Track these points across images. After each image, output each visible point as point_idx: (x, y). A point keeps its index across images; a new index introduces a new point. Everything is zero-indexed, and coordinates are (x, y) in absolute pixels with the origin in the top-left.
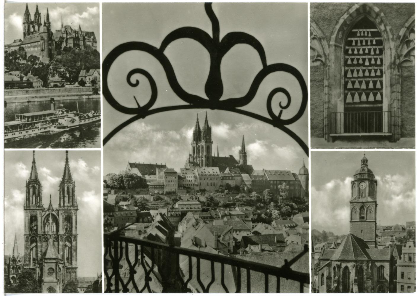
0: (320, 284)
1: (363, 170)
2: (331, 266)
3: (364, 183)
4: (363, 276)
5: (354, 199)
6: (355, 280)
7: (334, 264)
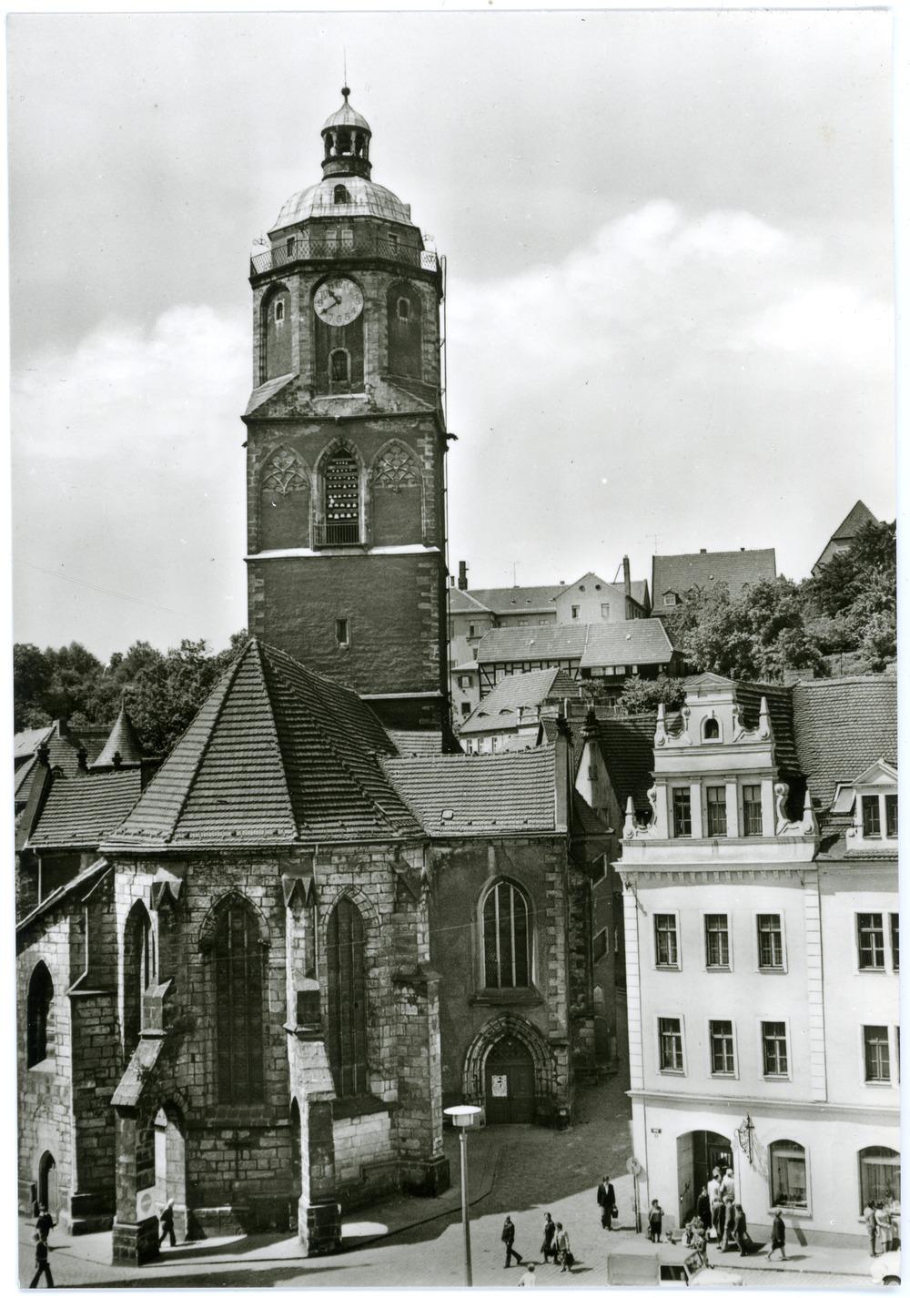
1: (341, 195)
2: (111, 900)
5: (274, 401)
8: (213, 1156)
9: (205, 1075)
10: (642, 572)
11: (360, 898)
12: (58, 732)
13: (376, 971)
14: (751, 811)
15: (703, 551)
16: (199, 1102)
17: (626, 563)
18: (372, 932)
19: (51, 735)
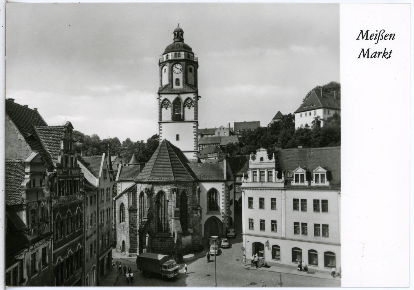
0: (118, 221)
2: (136, 191)
3: (179, 65)
4: (187, 206)
6: (176, 212)
7: (141, 188)
8: (157, 243)
9: (156, 226)
10: (232, 126)
11: (186, 192)
12: (118, 157)
13: (189, 207)
14: (270, 175)
15: (245, 121)
16: (154, 232)
17: (229, 124)
18: (189, 199)
19: (117, 158)
